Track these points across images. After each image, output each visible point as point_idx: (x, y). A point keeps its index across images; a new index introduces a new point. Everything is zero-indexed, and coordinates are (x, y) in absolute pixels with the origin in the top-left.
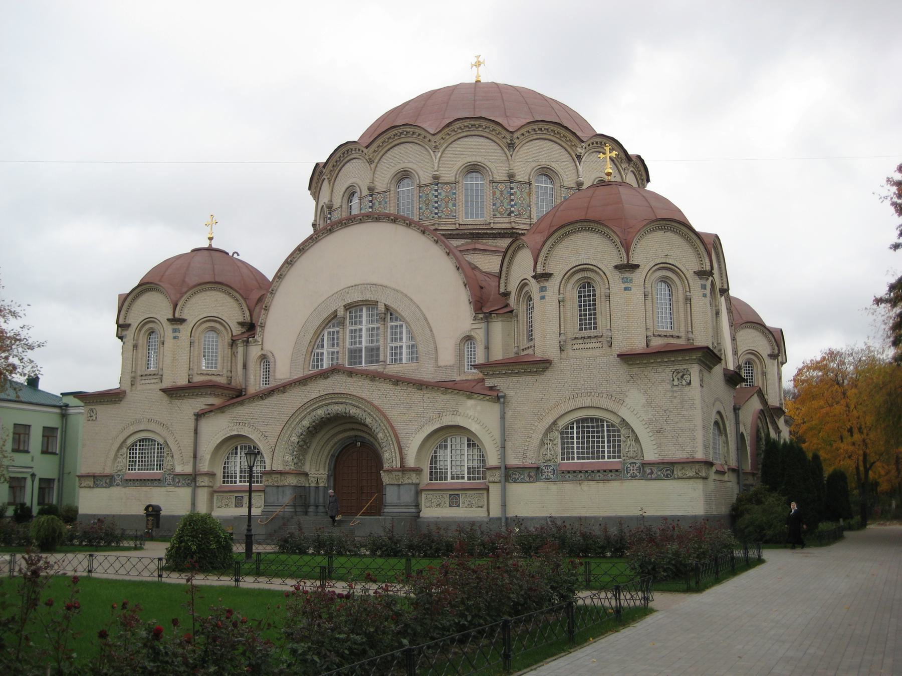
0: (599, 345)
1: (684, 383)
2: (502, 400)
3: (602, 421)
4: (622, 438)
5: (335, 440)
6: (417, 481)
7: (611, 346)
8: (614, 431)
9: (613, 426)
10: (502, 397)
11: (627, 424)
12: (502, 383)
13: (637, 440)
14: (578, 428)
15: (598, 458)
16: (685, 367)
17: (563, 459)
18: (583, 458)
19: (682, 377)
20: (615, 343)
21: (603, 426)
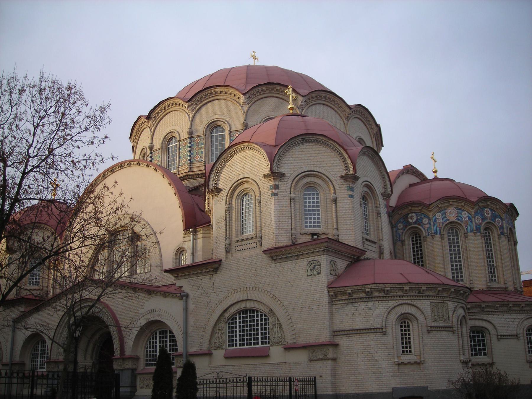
0: (254, 245)
1: (315, 272)
2: (184, 298)
3: (257, 312)
4: (271, 326)
5: (97, 337)
6: (134, 367)
7: (261, 245)
8: (265, 320)
9: (265, 316)
10: (184, 296)
11: (274, 314)
12: (185, 284)
13: (281, 327)
14: (240, 318)
15: (254, 344)
16: (315, 258)
17: (229, 346)
18: (244, 345)
19: (314, 268)
20: (264, 242)
21: (257, 316)
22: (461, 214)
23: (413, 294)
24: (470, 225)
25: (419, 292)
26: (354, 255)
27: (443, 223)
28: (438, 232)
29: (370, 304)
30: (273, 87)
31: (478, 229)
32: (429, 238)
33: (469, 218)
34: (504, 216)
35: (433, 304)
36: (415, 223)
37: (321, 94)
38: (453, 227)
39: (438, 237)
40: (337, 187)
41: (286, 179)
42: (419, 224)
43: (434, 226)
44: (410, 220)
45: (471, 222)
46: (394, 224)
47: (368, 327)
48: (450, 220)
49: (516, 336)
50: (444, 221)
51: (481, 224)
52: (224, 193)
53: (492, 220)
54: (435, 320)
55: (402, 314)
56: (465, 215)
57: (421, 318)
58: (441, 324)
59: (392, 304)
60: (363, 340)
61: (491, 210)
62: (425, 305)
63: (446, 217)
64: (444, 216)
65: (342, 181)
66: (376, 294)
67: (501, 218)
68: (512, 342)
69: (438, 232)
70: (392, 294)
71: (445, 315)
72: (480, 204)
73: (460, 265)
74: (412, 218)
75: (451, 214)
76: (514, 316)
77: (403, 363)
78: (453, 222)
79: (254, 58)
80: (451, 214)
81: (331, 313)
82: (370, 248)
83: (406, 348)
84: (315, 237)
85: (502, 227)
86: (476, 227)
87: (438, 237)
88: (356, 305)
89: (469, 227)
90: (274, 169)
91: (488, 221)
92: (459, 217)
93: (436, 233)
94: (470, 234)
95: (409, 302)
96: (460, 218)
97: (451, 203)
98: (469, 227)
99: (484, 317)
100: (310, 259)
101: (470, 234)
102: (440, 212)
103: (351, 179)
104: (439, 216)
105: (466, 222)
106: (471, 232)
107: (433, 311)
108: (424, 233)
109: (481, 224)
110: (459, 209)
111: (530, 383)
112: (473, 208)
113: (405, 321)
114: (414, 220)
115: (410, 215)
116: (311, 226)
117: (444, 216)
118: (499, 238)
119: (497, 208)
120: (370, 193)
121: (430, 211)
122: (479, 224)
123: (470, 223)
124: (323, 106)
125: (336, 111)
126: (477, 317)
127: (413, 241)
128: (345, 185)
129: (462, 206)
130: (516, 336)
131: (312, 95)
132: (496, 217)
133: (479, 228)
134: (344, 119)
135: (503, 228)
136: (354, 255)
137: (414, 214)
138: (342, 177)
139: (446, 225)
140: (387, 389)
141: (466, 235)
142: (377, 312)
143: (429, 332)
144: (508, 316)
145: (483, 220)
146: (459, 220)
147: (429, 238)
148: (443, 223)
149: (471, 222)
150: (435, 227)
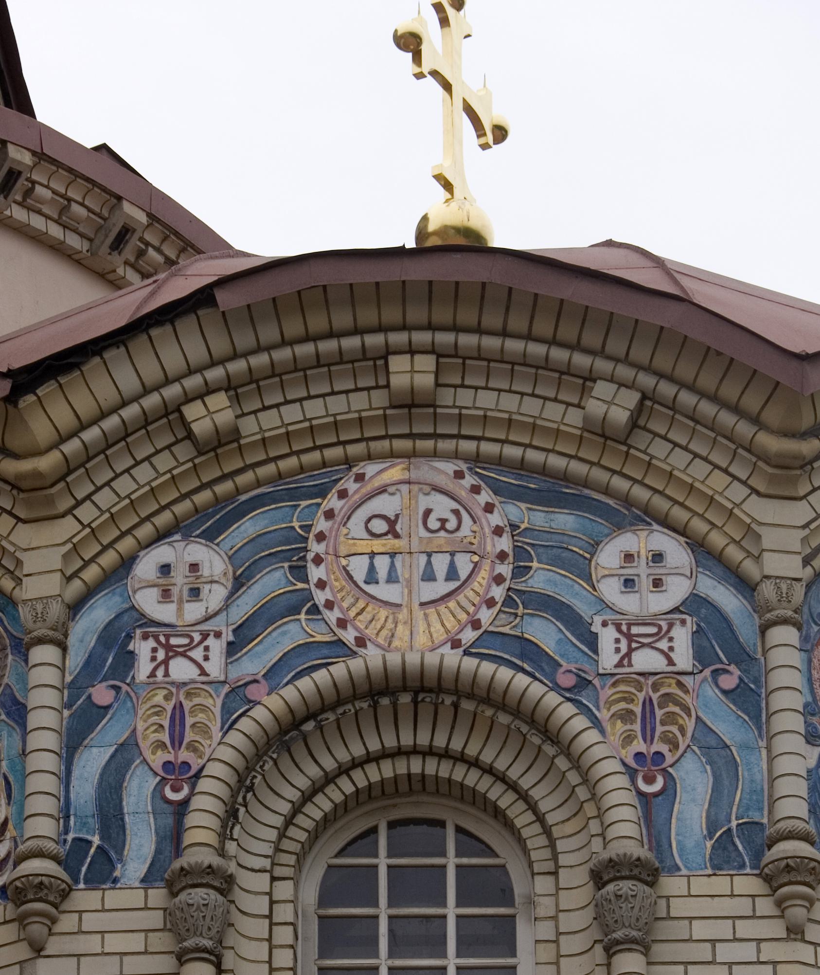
22: (583, 571)
24: (714, 749)
27: (238, 699)
28: (141, 845)
43: (73, 742)
50: (252, 665)
56: (641, 581)
63: (298, 604)
64: (272, 582)
69: (141, 845)
80: (408, 569)
89: (694, 780)
96: (544, 633)
97: (411, 373)
98: (694, 780)
102: (210, 524)
104: (186, 582)
105: (653, 705)
106: (723, 858)
110: (554, 490)
117: (272, 582)
123: (728, 725)
129: (600, 433)
139: (290, 734)
146: (529, 655)
148: (238, 699)
149: (750, 699)
150: (92, 761)
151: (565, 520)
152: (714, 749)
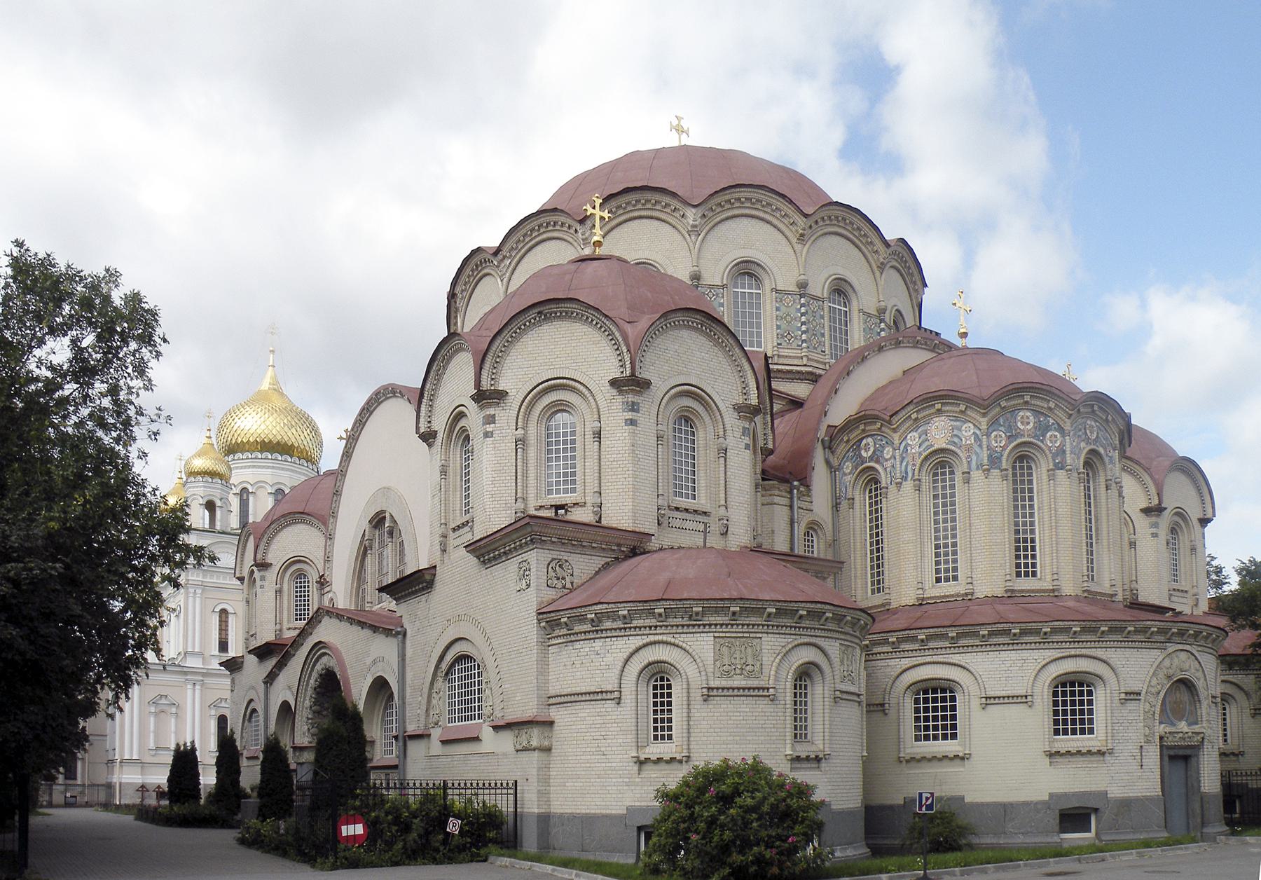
22: (960, 430)
23: (678, 621)
24: (977, 454)
25: (690, 618)
26: (619, 545)
27: (920, 454)
28: (910, 475)
29: (598, 643)
30: (638, 196)
31: (994, 461)
32: (893, 488)
33: (977, 438)
34: (1067, 426)
35: (722, 641)
36: (871, 458)
37: (737, 195)
38: (940, 462)
39: (908, 485)
40: (602, 404)
41: (509, 400)
42: (877, 462)
44: (864, 454)
45: (980, 446)
46: (835, 463)
47: (593, 689)
48: (936, 447)
49: (1023, 699)
51: (1004, 448)
52: (440, 435)
53: (1035, 437)
54: (726, 675)
55: (650, 664)
56: (968, 431)
57: (690, 670)
58: (738, 681)
59: (636, 642)
60: (586, 712)
61: (1036, 413)
62: (703, 644)
63: (927, 440)
65: (614, 392)
66: (608, 625)
67: (1061, 429)
68: (1014, 712)
69: (910, 475)
70: (635, 623)
71: (750, 661)
72: (1003, 404)
73: (954, 544)
74: (867, 449)
75: (939, 431)
76: (1025, 654)
77: (798, 759)
78: (942, 450)
79: (680, 130)
81: (543, 664)
82: (688, 525)
83: (662, 731)
84: (561, 512)
85: (1061, 451)
86: (990, 456)
87: (908, 485)
88: (577, 645)
89: (974, 458)
90: (484, 383)
91: (1026, 439)
92: (955, 435)
93: (905, 478)
94: (976, 475)
95: (669, 638)
96: (956, 440)
98: (974, 458)
99: (955, 659)
100: (555, 554)
101: (976, 475)
103: (631, 385)
105: (969, 448)
106: (978, 468)
107: (718, 656)
108: (884, 479)
109: (1004, 448)
111: (1046, 798)
112: (984, 415)
113: (659, 679)
114: (870, 453)
115: (864, 442)
116: (558, 492)
118: (1052, 478)
119: (1050, 409)
120: (700, 409)
121: (895, 430)
122: (999, 449)
123: (978, 450)
124: (745, 221)
125: (775, 227)
126: (940, 659)
127: (870, 498)
128: (620, 399)
129: (961, 412)
130: (1023, 699)
131: (717, 200)
132: (1047, 428)
133: (1000, 459)
134: (794, 240)
135: (1064, 451)
136: (619, 545)
137: (870, 440)
138: (614, 383)
139: (926, 458)
140: (617, 809)
141: (967, 481)
142: (609, 659)
143: (706, 698)
144: (1010, 656)
145: (1010, 438)
147: (893, 488)
149: (980, 446)
151: (958, 423)
152: (977, 454)
